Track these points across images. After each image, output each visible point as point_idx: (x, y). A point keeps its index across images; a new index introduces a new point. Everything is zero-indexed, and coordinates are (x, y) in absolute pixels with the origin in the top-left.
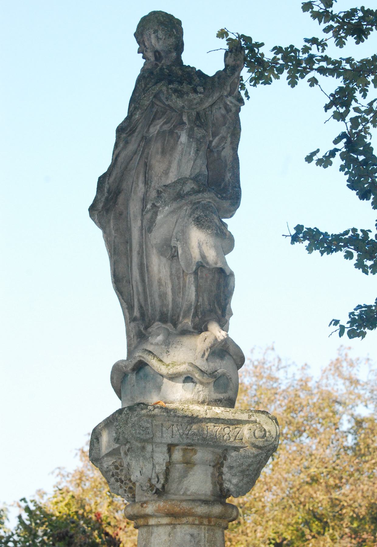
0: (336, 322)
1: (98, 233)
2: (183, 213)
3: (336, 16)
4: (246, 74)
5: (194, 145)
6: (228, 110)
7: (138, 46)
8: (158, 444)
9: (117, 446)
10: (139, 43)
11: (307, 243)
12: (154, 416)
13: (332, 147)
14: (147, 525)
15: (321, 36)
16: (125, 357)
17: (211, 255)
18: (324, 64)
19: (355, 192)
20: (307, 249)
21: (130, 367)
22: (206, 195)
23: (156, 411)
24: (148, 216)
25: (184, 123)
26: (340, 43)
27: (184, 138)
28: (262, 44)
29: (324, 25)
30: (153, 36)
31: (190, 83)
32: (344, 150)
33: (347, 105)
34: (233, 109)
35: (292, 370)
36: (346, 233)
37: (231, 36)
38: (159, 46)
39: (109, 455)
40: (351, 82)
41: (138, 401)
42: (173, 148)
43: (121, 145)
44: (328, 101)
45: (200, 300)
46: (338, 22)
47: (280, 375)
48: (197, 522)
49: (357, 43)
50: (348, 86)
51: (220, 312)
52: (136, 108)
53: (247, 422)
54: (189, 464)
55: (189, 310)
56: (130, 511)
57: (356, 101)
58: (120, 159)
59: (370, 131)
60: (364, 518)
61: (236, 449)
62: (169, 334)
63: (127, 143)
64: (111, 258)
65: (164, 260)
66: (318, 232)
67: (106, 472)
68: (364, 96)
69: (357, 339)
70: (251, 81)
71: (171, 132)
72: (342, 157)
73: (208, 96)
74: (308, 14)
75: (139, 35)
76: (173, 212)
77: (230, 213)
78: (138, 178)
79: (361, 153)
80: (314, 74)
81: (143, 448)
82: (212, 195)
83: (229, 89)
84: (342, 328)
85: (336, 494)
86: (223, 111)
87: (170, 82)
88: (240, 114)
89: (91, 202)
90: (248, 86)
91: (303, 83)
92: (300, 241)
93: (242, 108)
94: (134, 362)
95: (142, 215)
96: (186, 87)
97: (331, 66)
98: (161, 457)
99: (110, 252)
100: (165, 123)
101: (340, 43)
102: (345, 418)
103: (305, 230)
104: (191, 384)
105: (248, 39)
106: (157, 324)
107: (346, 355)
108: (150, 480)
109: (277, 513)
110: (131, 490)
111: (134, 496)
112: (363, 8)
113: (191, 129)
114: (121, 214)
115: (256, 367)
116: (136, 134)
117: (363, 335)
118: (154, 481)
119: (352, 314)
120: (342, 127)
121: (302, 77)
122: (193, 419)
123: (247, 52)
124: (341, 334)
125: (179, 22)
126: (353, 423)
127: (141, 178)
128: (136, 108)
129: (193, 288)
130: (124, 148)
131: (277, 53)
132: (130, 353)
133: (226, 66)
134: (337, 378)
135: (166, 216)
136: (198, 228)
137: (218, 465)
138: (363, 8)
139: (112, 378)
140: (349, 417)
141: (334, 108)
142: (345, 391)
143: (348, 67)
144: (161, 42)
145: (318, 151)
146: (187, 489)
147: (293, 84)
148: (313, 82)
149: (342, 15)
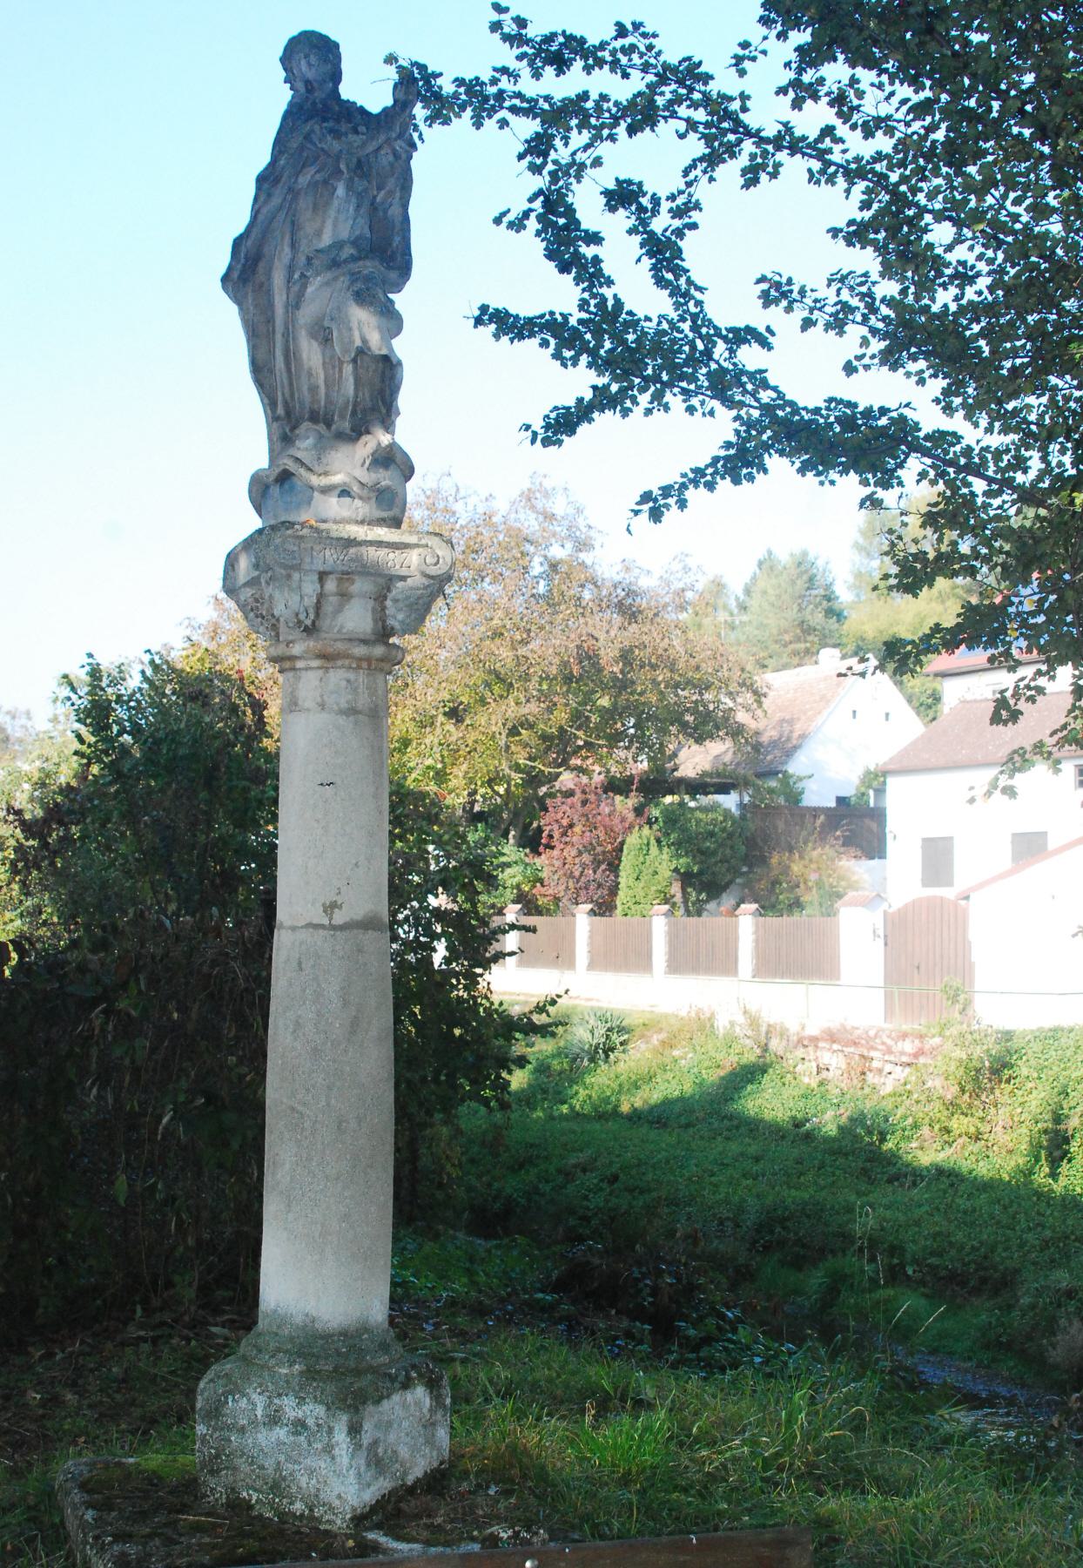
0: (528, 427)
1: (233, 309)
2: (339, 284)
3: (532, 40)
4: (420, 112)
5: (354, 200)
6: (396, 155)
7: (284, 74)
8: (307, 572)
9: (257, 573)
10: (285, 69)
11: (493, 327)
12: (302, 537)
13: (527, 206)
14: (293, 669)
15: (513, 64)
16: (266, 465)
17: (375, 340)
18: (517, 102)
19: (553, 264)
20: (494, 336)
21: (272, 479)
22: (368, 263)
23: (305, 532)
24: (296, 288)
25: (341, 172)
26: (537, 75)
27: (341, 191)
28: (441, 75)
29: (516, 52)
30: (303, 62)
31: (350, 121)
32: (541, 211)
33: (545, 155)
34: (404, 156)
35: (472, 501)
36: (542, 316)
37: (401, 62)
38: (310, 75)
39: (247, 584)
40: (550, 127)
41: (283, 519)
42: (327, 204)
43: (262, 199)
44: (522, 149)
45: (361, 394)
46: (534, 47)
47: (458, 507)
48: (354, 665)
49: (558, 75)
50: (546, 131)
51: (384, 411)
52: (281, 152)
53: (417, 546)
54: (345, 596)
55: (346, 407)
56: (274, 652)
57: (556, 150)
58: (261, 217)
59: (572, 188)
60: (555, 678)
61: (403, 578)
62: (321, 437)
63: (269, 195)
64: (248, 341)
65: (315, 344)
66: (508, 315)
67: (244, 606)
68: (566, 144)
69: (552, 448)
70: (425, 121)
71: (325, 182)
72: (540, 218)
73: (372, 139)
74: (497, 36)
75: (287, 60)
76: (327, 284)
77: (398, 288)
78: (283, 238)
79: (561, 215)
80: (504, 114)
81: (289, 577)
82: (377, 263)
83: (398, 130)
84: (535, 434)
85: (522, 651)
86: (391, 158)
87: (325, 120)
88: (412, 162)
89: (223, 270)
90: (422, 127)
91: (490, 124)
92: (485, 325)
93: (415, 154)
94: (277, 471)
95: (288, 288)
96: (344, 127)
97: (525, 105)
98: (310, 588)
99: (247, 333)
100: (318, 172)
101: (537, 75)
102: (537, 560)
103: (491, 310)
104: (348, 500)
105: (422, 67)
106: (306, 425)
107: (541, 484)
108: (297, 615)
109: (452, 671)
110: (275, 627)
111: (277, 635)
112: (564, 32)
113: (351, 180)
114: (261, 285)
115: (428, 497)
116: (281, 184)
117: (560, 443)
118: (302, 617)
119: (547, 416)
120: (541, 182)
121: (490, 117)
122: (351, 542)
123: (421, 83)
124: (533, 441)
125: (337, 46)
126: (546, 567)
127: (287, 240)
128: (281, 152)
129: (351, 380)
130: (266, 202)
131: (459, 86)
132: (274, 456)
133: (395, 101)
134: (529, 512)
135: (317, 290)
136: (357, 304)
137: (380, 598)
138: (564, 32)
139: (250, 492)
140: (542, 559)
141: (529, 158)
142: (537, 528)
143: (546, 106)
144: (313, 70)
145: (509, 211)
146: (342, 627)
147: (478, 125)
148: (503, 123)
149: (538, 39)
